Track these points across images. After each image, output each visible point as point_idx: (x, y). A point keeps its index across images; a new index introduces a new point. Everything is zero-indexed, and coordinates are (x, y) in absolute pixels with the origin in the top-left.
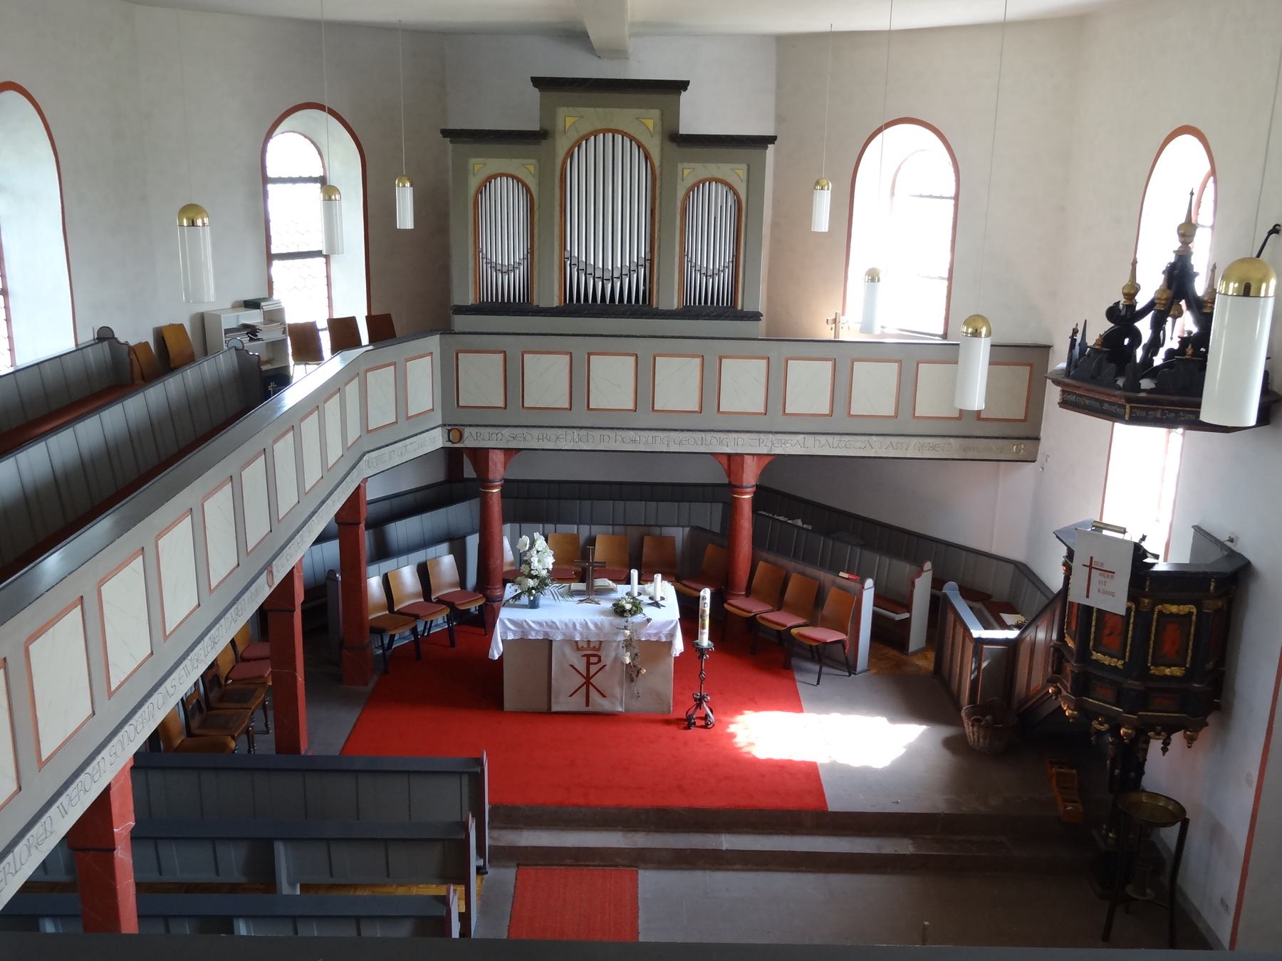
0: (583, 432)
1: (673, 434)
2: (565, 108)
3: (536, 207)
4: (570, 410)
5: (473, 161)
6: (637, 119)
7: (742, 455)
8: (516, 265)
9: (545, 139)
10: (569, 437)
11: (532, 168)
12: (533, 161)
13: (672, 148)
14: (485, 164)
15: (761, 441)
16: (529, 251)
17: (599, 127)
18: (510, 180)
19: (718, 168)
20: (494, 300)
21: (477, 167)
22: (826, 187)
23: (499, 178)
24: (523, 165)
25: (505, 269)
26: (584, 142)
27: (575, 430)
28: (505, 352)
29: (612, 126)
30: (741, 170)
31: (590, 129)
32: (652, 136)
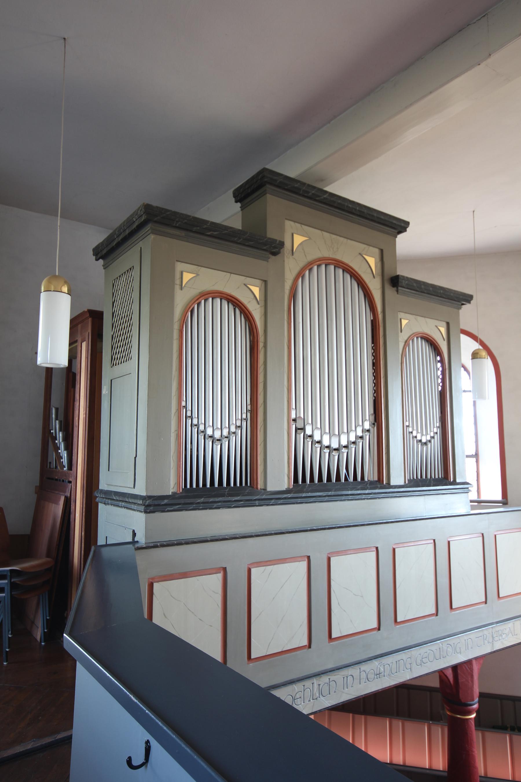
0: (325, 679)
1: (414, 652)
2: (292, 223)
3: (261, 345)
4: (310, 646)
5: (180, 266)
6: (360, 254)
7: (469, 662)
8: (233, 429)
9: (275, 254)
10: (308, 692)
11: (256, 290)
12: (258, 282)
13: (390, 291)
14: (198, 275)
15: (485, 637)
16: (249, 408)
17: (327, 254)
18: (225, 303)
19: (426, 322)
20: (208, 485)
21: (187, 277)
22: (486, 358)
23: (211, 299)
24: (245, 285)
25: (217, 435)
26: (307, 272)
27: (315, 680)
28: (225, 569)
29: (338, 257)
30: (443, 330)
31: (318, 255)
32: (374, 277)
